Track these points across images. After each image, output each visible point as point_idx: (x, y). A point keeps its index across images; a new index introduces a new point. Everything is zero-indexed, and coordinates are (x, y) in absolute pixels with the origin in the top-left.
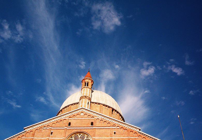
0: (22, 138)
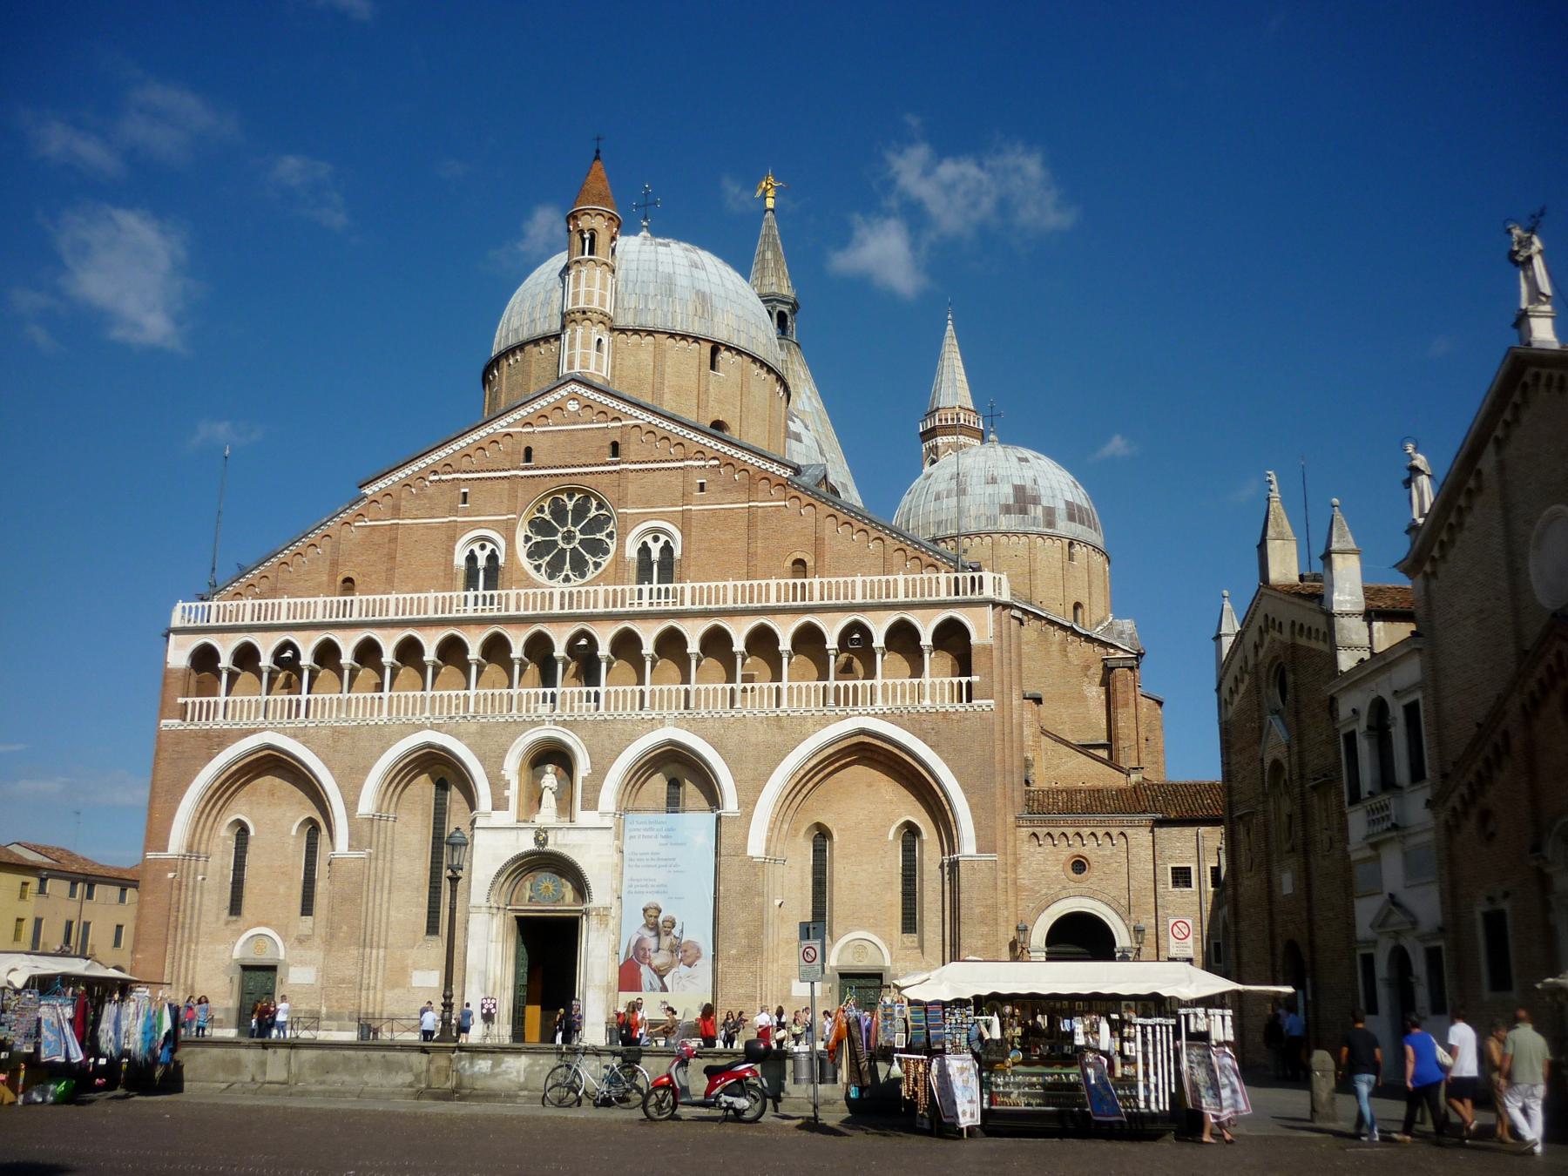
0: (357, 524)
